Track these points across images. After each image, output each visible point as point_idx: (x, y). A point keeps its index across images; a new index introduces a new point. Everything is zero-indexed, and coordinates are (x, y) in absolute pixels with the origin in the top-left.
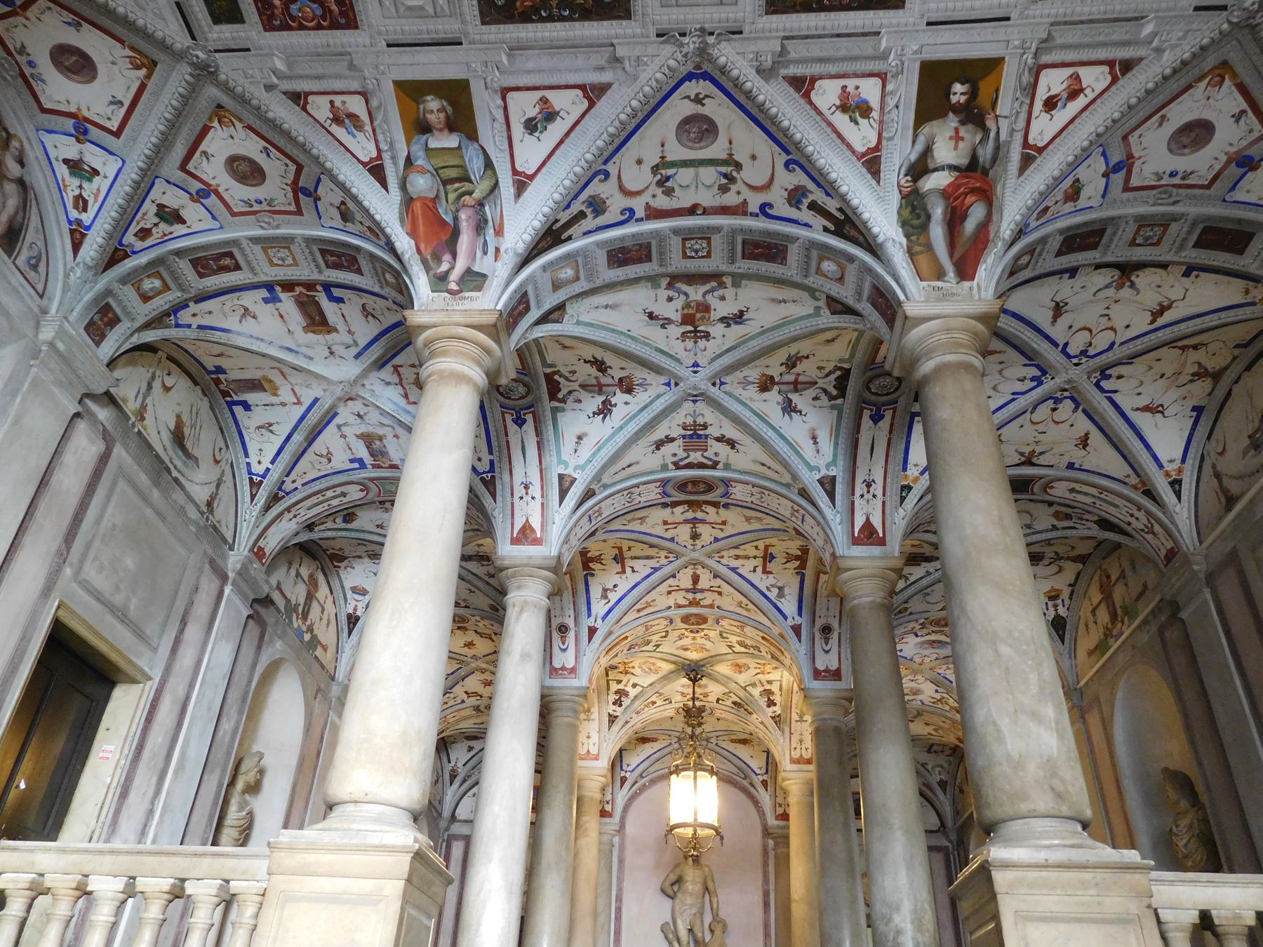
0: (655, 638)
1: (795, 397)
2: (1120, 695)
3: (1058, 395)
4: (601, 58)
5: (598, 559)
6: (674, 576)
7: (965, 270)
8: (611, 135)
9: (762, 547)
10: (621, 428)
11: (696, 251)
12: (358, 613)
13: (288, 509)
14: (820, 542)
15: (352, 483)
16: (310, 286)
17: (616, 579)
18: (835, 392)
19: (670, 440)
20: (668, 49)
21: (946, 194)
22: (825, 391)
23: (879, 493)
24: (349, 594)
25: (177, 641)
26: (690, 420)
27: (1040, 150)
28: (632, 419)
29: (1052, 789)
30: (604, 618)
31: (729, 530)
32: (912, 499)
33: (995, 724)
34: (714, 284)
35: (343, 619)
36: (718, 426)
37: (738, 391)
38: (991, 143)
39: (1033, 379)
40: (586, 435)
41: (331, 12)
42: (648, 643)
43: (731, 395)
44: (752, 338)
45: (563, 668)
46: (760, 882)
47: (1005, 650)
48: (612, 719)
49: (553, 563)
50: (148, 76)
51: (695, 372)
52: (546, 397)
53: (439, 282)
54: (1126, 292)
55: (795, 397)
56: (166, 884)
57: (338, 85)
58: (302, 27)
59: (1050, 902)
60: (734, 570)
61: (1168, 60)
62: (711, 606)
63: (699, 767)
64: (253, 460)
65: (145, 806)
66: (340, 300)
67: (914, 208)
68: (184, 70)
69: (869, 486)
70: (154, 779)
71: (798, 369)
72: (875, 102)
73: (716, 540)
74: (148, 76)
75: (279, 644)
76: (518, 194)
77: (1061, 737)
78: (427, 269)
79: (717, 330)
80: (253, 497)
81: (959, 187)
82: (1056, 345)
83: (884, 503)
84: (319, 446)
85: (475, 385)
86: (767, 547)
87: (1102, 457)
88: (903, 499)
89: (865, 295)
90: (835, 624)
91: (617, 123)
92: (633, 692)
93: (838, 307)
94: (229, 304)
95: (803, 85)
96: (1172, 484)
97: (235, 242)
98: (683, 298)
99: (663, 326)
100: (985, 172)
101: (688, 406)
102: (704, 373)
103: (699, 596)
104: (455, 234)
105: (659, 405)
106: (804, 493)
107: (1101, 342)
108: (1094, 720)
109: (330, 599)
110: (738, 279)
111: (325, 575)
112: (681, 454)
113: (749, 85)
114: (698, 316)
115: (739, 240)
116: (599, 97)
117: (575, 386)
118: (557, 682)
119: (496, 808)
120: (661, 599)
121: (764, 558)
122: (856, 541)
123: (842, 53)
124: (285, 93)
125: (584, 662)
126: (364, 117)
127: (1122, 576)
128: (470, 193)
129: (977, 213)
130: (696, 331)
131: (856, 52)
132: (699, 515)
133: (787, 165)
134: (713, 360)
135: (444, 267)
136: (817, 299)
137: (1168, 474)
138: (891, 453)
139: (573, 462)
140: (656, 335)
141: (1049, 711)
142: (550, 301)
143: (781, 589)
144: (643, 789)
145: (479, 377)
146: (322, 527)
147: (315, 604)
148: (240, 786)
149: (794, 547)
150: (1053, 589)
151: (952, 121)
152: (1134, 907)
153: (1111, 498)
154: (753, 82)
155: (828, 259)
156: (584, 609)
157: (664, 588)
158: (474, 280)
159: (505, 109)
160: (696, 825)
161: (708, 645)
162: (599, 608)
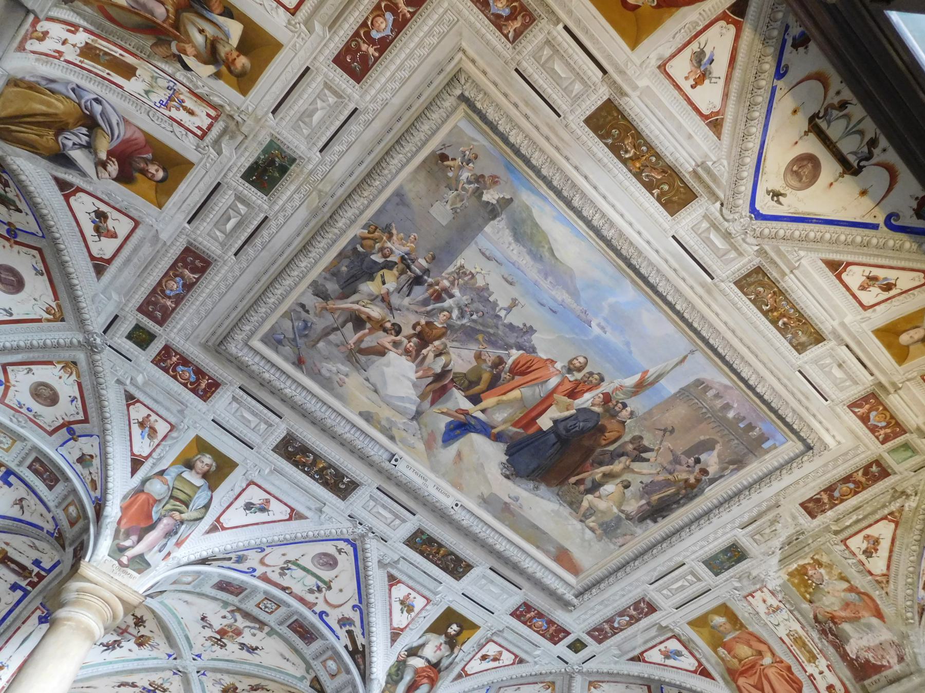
4: (314, 505)
8: (285, 539)
10: (111, 663)
11: (266, 607)
20: (349, 524)
21: (417, 671)
27: (467, 675)
28: (123, 661)
34: (257, 626)
38: (450, 659)
41: (199, 385)
43: (201, 682)
44: (250, 664)
50: (49, 320)
51: (194, 659)
57: (162, 412)
58: (175, 377)
61: (537, 669)
67: (398, 669)
68: (78, 337)
72: (417, 609)
74: (49, 320)
76: (208, 532)
81: (424, 671)
91: (293, 536)
95: (393, 580)
98: (232, 621)
99: (204, 627)
100: (439, 671)
101: (168, 674)
102: (199, 663)
104: (152, 527)
110: (272, 632)
113: (370, 564)
115: (295, 618)
116: (296, 519)
123: (421, 580)
124: (125, 391)
126: (160, 436)
128: (181, 512)
131: (426, 584)
133: (354, 607)
134: (213, 659)
135: (128, 543)
136: (308, 672)
151: (442, 639)
154: (373, 564)
155: (335, 661)
158: (141, 563)
159: (244, 490)
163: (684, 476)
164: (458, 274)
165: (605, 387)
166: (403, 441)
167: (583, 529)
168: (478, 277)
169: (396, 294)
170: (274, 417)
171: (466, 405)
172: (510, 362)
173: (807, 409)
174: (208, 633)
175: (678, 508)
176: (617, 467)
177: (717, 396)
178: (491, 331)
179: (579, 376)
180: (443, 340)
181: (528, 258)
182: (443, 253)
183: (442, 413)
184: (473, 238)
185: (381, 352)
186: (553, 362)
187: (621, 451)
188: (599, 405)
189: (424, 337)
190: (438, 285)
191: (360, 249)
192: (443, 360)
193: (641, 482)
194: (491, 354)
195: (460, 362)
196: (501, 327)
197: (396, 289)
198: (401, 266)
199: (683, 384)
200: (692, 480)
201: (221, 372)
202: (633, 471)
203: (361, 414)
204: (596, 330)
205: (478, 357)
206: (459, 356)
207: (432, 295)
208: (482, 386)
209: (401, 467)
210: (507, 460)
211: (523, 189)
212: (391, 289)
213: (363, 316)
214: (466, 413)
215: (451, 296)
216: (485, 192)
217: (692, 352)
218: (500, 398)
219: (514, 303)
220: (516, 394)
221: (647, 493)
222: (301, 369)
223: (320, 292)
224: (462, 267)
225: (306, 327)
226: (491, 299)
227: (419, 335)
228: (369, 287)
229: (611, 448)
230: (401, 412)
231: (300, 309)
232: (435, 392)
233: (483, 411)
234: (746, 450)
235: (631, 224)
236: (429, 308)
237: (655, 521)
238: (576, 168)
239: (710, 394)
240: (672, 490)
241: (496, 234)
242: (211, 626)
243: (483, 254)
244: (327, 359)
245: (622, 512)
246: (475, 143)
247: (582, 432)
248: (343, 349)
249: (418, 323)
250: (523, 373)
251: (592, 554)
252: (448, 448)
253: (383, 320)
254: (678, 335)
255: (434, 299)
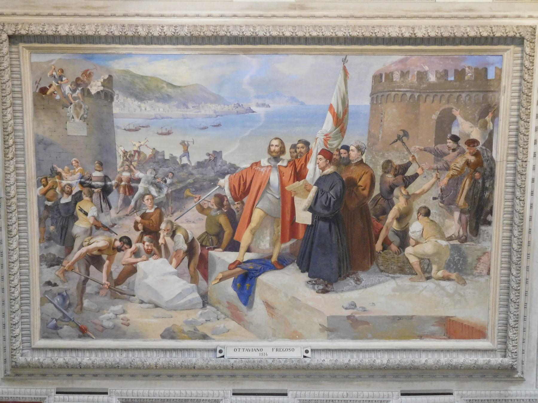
163: (460, 162)
164: (127, 160)
165: (316, 147)
166: (216, 332)
167: (439, 285)
168: (142, 150)
169: (102, 215)
170: (101, 397)
171: (231, 257)
172: (227, 192)
173: (481, 17)
175: (492, 193)
176: (400, 203)
177: (404, 74)
178: (190, 181)
179: (287, 157)
180: (165, 219)
181: (160, 104)
182: (104, 154)
183: (221, 280)
184: (113, 125)
185: (131, 270)
186: (258, 164)
187: (387, 187)
188: (327, 165)
189: (151, 231)
190: (122, 181)
191: (49, 204)
192: (180, 236)
193: (434, 199)
194: (208, 198)
195: (193, 225)
196: (194, 172)
197: (98, 211)
198: (85, 190)
199: (369, 91)
200: (472, 159)
201: (33, 391)
202: (416, 196)
203: (163, 337)
204: (260, 111)
205: (202, 209)
206: (188, 221)
207: (125, 193)
208: (228, 231)
209: (229, 354)
210: (309, 276)
211: (111, 62)
212: (95, 214)
213: (95, 253)
214: (237, 264)
215: (138, 181)
216: (89, 87)
217: (345, 61)
218: (250, 227)
219: (185, 146)
220: (257, 214)
221: (450, 204)
222: (89, 336)
223: (53, 262)
224: (125, 153)
225: (64, 298)
226: (167, 157)
227: (146, 231)
228: (80, 227)
229: (377, 191)
230: (190, 307)
231: (49, 288)
232: (198, 267)
233: (249, 250)
234: (481, 95)
235: (198, 16)
236: (133, 204)
237: (489, 223)
238: (125, 16)
239: (397, 77)
240: (467, 183)
241: (124, 109)
243: (130, 130)
244: (99, 311)
245: (450, 239)
246: (53, 63)
247: (340, 199)
248: (103, 292)
249: (136, 223)
250: (246, 192)
251: (473, 303)
252: (255, 306)
253: (110, 242)
254: (320, 59)
255: (130, 194)
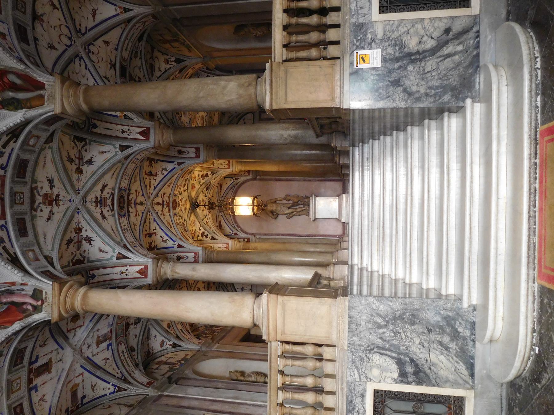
0: (182, 221)
1: (85, 160)
2: (207, 44)
3: (87, 51)
5: (150, 244)
6: (157, 213)
7: (41, 86)
9: (146, 176)
10: (97, 233)
11: (21, 198)
12: (172, 343)
13: (130, 374)
14: (147, 153)
15: (118, 349)
16: (30, 371)
17: (158, 236)
18: (84, 143)
19: (102, 213)
22: (83, 147)
23: (127, 128)
24: (163, 348)
25: (188, 408)
26: (94, 204)
28: (93, 229)
29: (248, 86)
30: (174, 241)
31: (139, 189)
32: (129, 114)
33: (227, 101)
34: (35, 191)
35: (174, 349)
36: (96, 192)
37: (82, 183)
39: (80, 61)
40: (99, 248)
42: (183, 223)
43: (83, 186)
44: (60, 176)
45: (195, 257)
46: (273, 182)
47: (201, 94)
48: (213, 238)
49: (155, 260)
51: (73, 201)
52: (83, 265)
53: (37, 309)
54: (45, 18)
55: (85, 160)
56: (279, 376)
59: (281, 93)
60: (155, 188)
62: (169, 198)
63: (232, 204)
64: (108, 392)
65: (251, 407)
66: (37, 358)
69: (124, 132)
70: (241, 406)
71: (73, 157)
73: (143, 195)
75: (186, 372)
77: (231, 80)
78: (30, 315)
79: (55, 191)
80: (125, 390)
82: (66, 50)
83: (131, 126)
84: (101, 363)
85: (87, 290)
86: (146, 174)
87: (114, 36)
88: (130, 119)
89: (46, 127)
90: (177, 148)
92: (202, 230)
93: (49, 140)
94: (38, 408)
96: (126, 12)
97: (9, 407)
98: (41, 205)
99: (53, 214)
101: (88, 204)
102: (74, 197)
103: (165, 203)
104: (13, 303)
105: (87, 217)
106: (126, 158)
107: (65, 31)
108: (215, 54)
109: (166, 356)
110: (34, 181)
111: (156, 358)
112: (108, 208)
114: (49, 199)
115: (16, 179)
117: (78, 253)
118: (200, 259)
119: (250, 276)
120: (166, 218)
121: (150, 175)
122: (148, 139)
125: (192, 248)
127: (161, 35)
129: (12, 78)
130: (56, 200)
132: (133, 201)
134: (68, 193)
135: (30, 307)
136: (45, 148)
137: (121, 12)
138: (110, 121)
139: (112, 254)
140: (57, 217)
141: (223, 83)
142: (44, 262)
143: (163, 169)
144: (239, 226)
145: (82, 290)
146: (137, 360)
147: (169, 361)
148: (242, 378)
149: (146, 164)
150: (164, 61)
152: (282, 68)
153: (130, 35)
155: (29, 141)
156: (170, 249)
157: (162, 217)
158: (37, 294)
160: (253, 205)
161: (184, 199)
162: (170, 243)
174: (55, 209)
242: (51, 211)
